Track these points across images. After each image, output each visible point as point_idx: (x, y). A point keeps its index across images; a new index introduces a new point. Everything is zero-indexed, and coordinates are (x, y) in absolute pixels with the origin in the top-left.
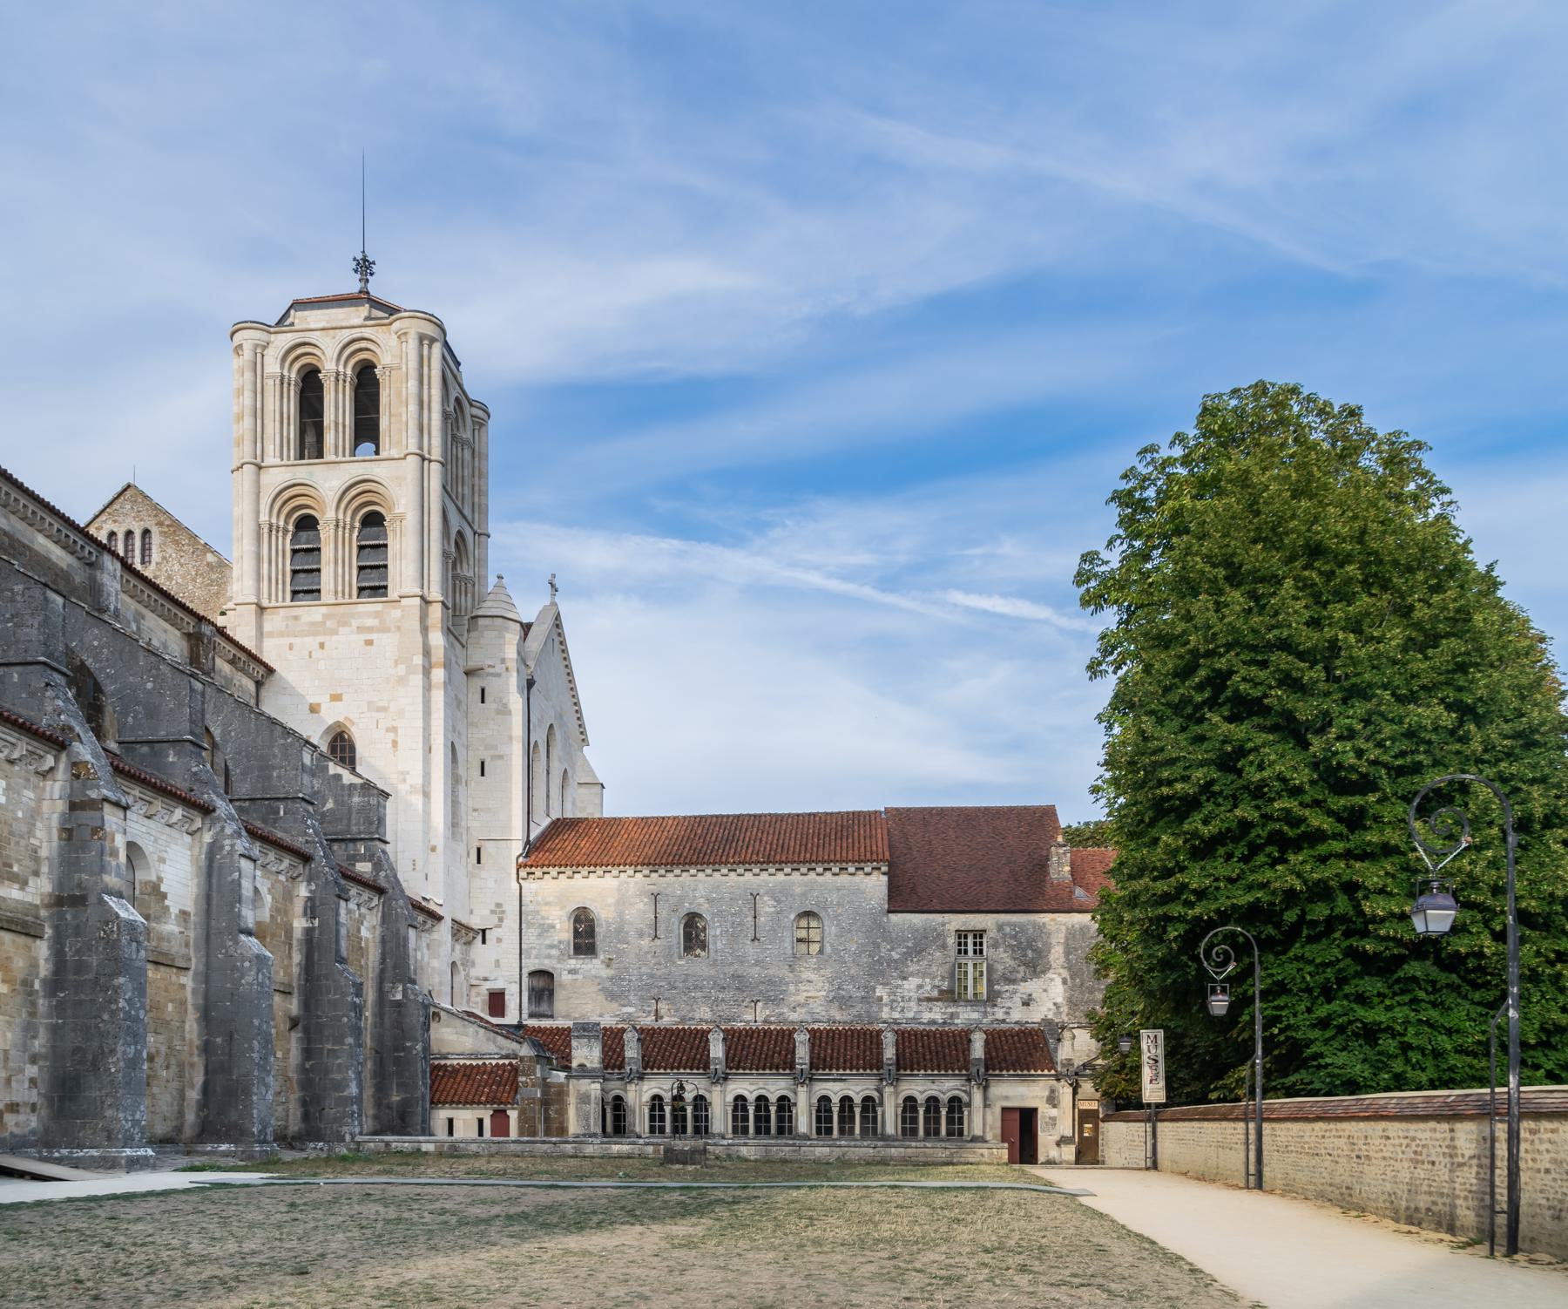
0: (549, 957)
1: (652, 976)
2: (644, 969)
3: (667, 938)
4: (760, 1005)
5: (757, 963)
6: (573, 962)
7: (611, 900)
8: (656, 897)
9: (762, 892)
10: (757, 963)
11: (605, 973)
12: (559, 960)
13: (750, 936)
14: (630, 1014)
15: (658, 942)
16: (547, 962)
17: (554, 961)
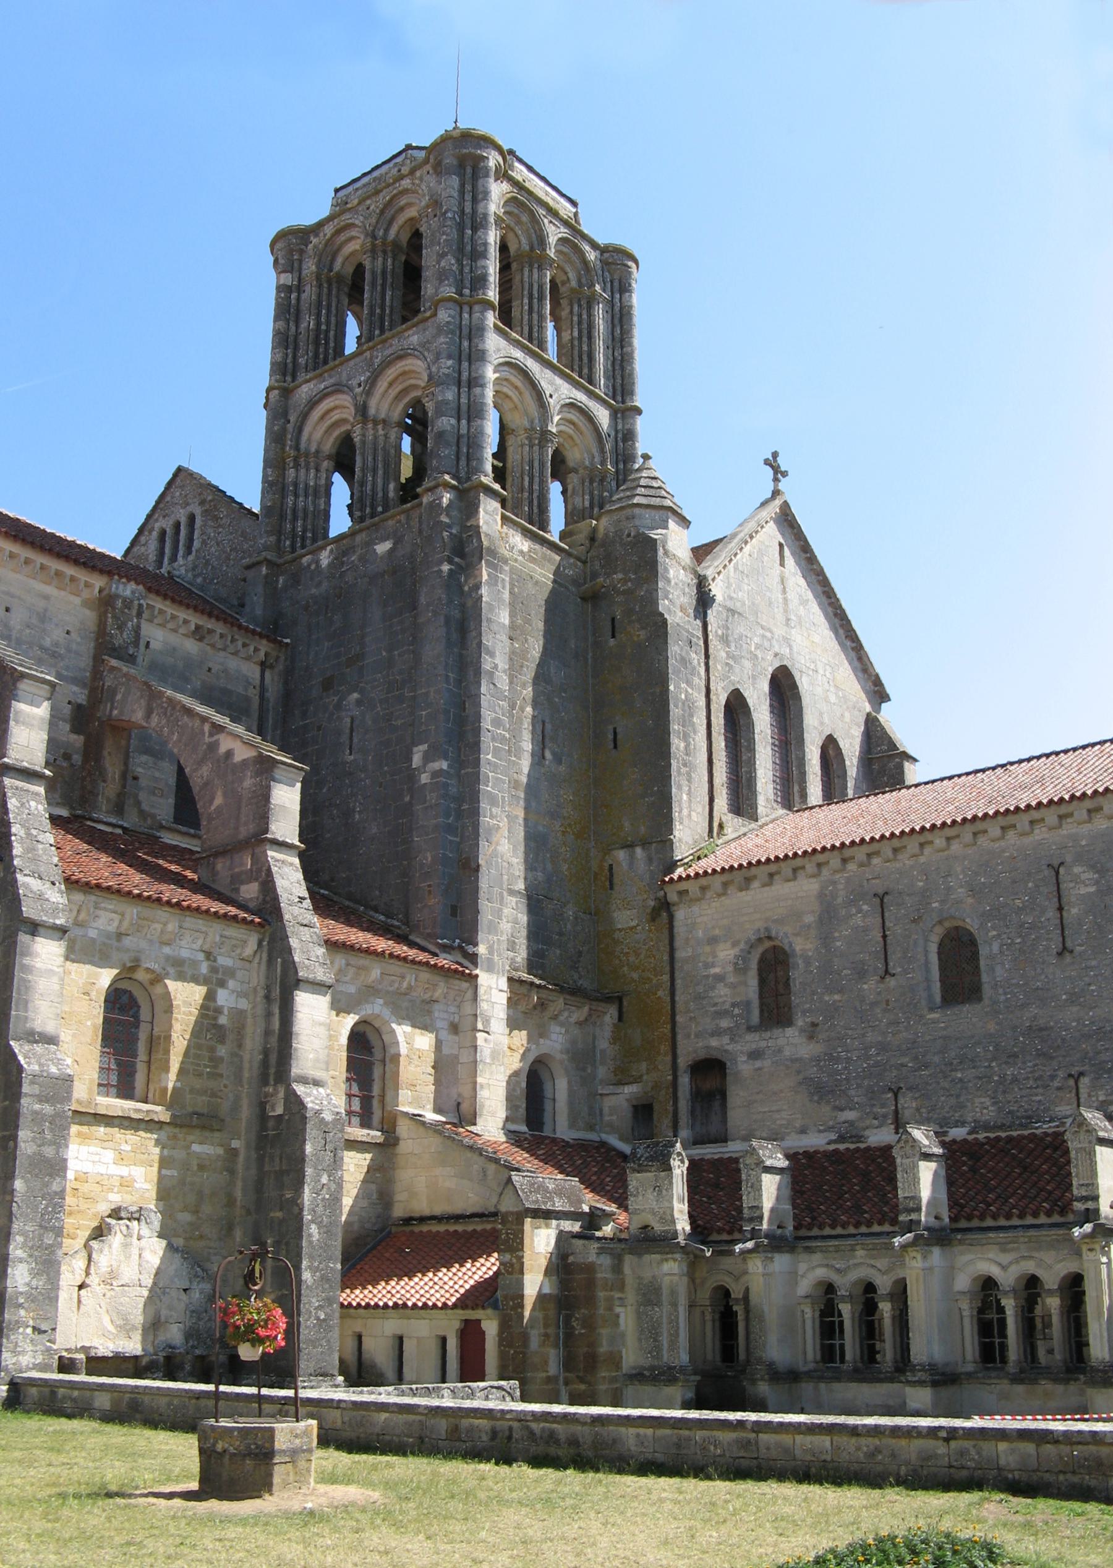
0: (717, 1033)
1: (883, 1047)
2: (871, 1037)
3: (906, 972)
4: (1085, 1081)
5: (1074, 998)
6: (755, 1036)
7: (809, 919)
8: (881, 898)
9: (1068, 858)
10: (1074, 998)
11: (806, 1050)
12: (733, 1034)
13: (1055, 946)
14: (851, 1123)
15: (892, 982)
16: (714, 1042)
17: (726, 1039)
